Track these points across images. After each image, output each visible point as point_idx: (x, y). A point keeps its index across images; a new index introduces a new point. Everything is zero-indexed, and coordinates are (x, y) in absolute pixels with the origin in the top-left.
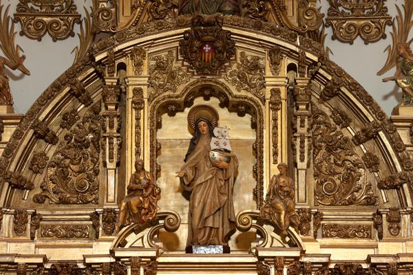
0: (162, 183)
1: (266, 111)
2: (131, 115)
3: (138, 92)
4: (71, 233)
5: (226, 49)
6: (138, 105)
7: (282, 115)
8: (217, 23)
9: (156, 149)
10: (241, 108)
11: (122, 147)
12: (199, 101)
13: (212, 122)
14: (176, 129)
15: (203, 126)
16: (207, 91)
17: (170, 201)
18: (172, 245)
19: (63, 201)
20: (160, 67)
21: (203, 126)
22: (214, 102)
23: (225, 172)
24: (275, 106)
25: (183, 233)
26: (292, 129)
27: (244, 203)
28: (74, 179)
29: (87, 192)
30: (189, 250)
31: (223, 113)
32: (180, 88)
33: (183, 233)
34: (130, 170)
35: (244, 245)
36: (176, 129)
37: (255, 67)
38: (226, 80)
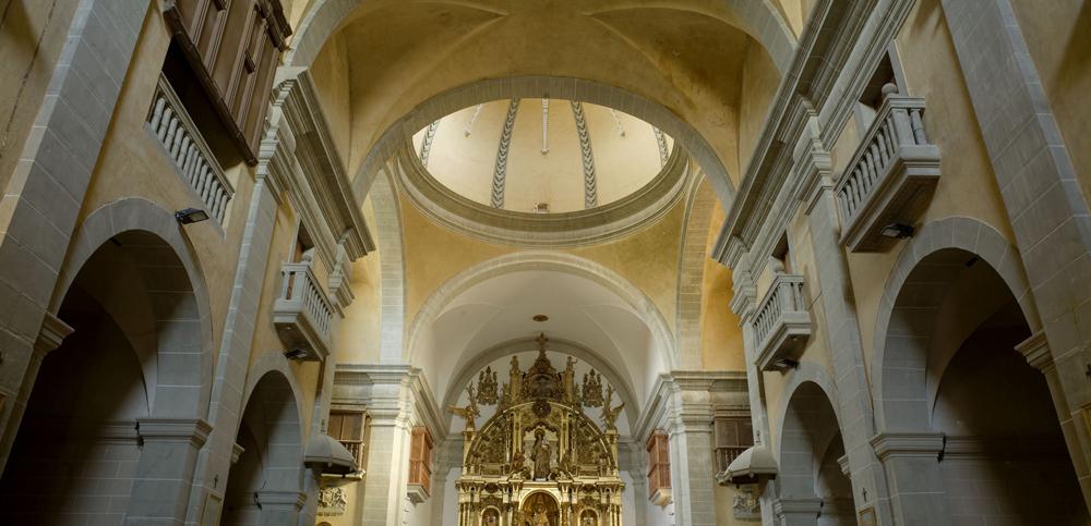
0: (525, 456)
1: (562, 432)
2: (515, 431)
3: (517, 424)
4: (494, 473)
5: (547, 409)
6: (517, 429)
7: (567, 432)
8: (545, 400)
9: (523, 444)
10: (553, 430)
11: (512, 443)
12: (538, 427)
13: (542, 436)
14: (530, 436)
15: (540, 436)
16: (541, 424)
17: (528, 463)
18: (528, 478)
19: (491, 462)
20: (525, 415)
21: (540, 436)
22: (544, 427)
23: (547, 454)
24: (564, 429)
25: (532, 474)
26: (570, 437)
27: (553, 464)
28: (495, 454)
29: (500, 459)
30: (534, 480)
31: (547, 431)
32: (532, 423)
33: (532, 474)
34: (514, 451)
35: (553, 477)
36: (530, 436)
37: (558, 415)
38: (548, 420)
